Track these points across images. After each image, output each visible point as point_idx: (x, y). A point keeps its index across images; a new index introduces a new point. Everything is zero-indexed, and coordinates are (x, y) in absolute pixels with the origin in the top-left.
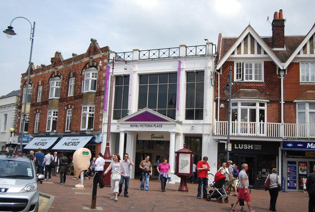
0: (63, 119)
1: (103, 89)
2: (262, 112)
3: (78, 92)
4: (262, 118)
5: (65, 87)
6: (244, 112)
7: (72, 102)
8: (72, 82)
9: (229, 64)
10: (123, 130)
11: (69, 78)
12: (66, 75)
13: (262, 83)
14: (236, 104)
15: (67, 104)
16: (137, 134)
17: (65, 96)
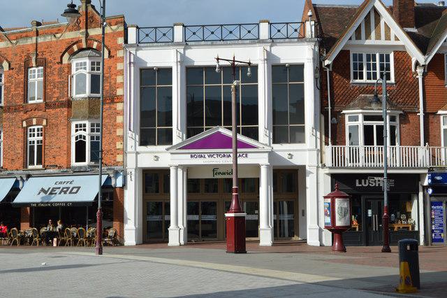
0: (19, 145)
1: (119, 92)
2: (393, 129)
3: (56, 95)
4: (393, 143)
5: (17, 85)
6: (368, 130)
7: (40, 113)
8: (36, 77)
9: (344, 54)
10: (177, 163)
11: (27, 66)
12: (18, 62)
13: (392, 84)
14: (356, 119)
15: (26, 116)
16: (188, 169)
17: (19, 101)
